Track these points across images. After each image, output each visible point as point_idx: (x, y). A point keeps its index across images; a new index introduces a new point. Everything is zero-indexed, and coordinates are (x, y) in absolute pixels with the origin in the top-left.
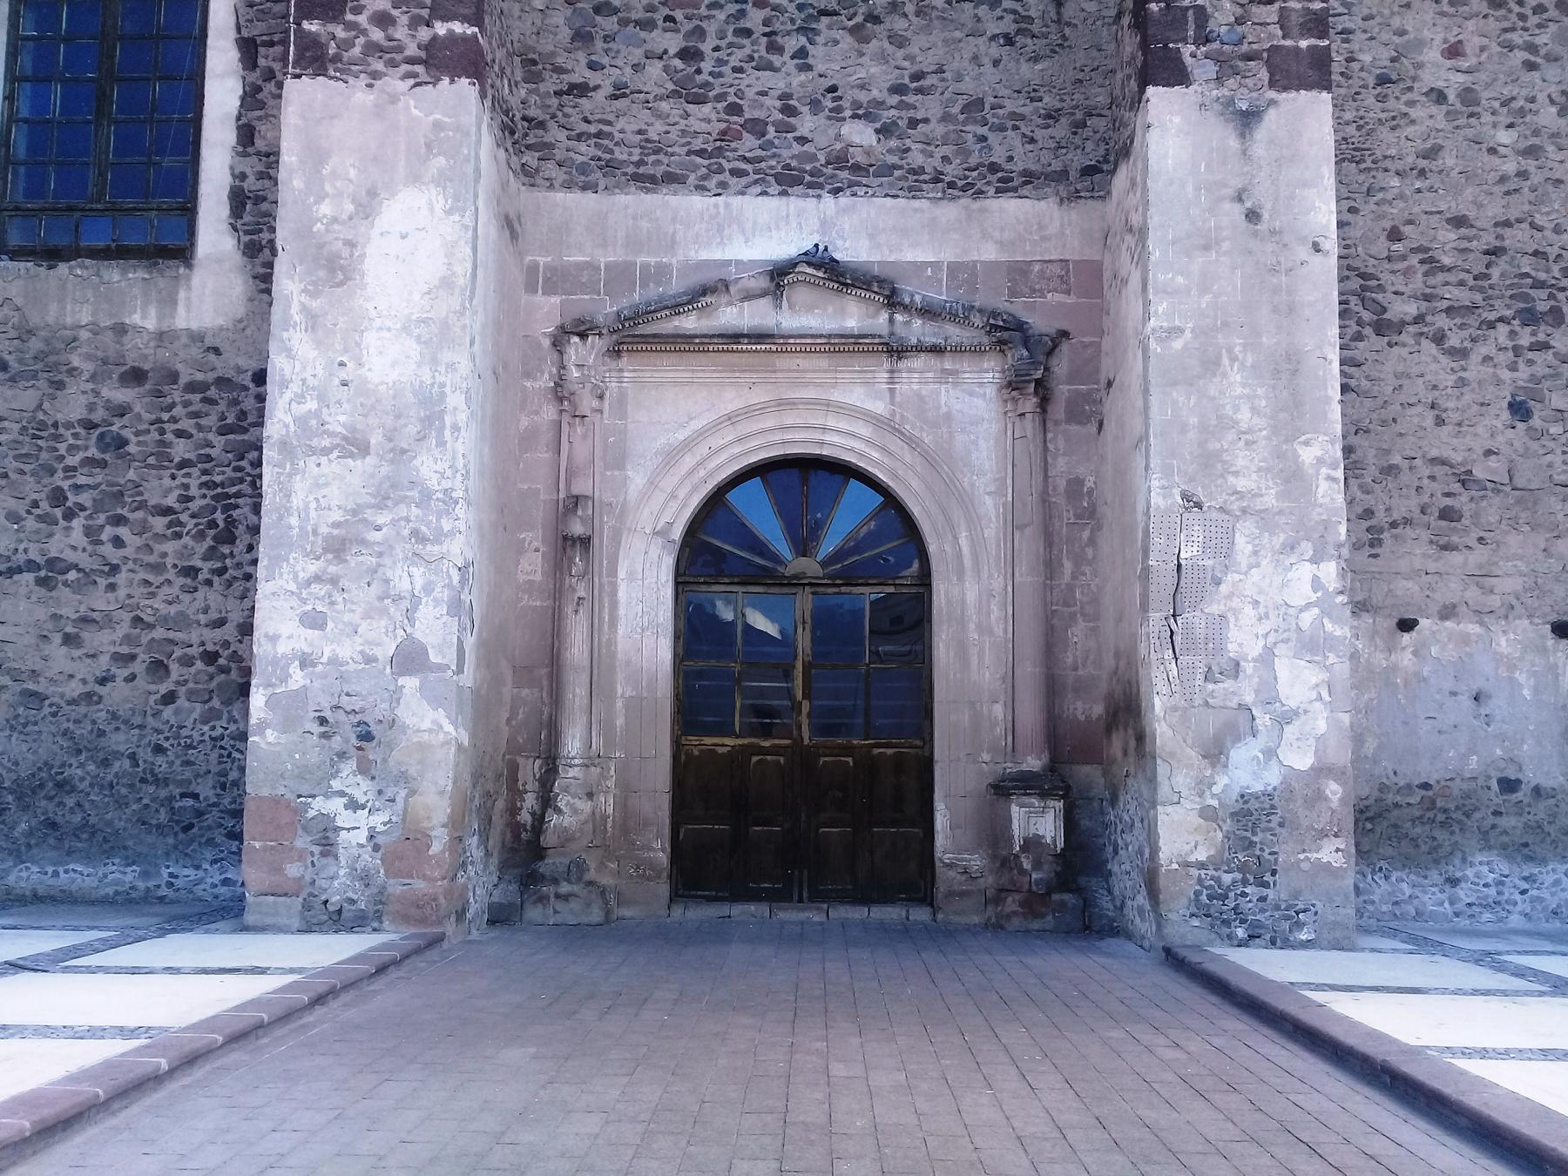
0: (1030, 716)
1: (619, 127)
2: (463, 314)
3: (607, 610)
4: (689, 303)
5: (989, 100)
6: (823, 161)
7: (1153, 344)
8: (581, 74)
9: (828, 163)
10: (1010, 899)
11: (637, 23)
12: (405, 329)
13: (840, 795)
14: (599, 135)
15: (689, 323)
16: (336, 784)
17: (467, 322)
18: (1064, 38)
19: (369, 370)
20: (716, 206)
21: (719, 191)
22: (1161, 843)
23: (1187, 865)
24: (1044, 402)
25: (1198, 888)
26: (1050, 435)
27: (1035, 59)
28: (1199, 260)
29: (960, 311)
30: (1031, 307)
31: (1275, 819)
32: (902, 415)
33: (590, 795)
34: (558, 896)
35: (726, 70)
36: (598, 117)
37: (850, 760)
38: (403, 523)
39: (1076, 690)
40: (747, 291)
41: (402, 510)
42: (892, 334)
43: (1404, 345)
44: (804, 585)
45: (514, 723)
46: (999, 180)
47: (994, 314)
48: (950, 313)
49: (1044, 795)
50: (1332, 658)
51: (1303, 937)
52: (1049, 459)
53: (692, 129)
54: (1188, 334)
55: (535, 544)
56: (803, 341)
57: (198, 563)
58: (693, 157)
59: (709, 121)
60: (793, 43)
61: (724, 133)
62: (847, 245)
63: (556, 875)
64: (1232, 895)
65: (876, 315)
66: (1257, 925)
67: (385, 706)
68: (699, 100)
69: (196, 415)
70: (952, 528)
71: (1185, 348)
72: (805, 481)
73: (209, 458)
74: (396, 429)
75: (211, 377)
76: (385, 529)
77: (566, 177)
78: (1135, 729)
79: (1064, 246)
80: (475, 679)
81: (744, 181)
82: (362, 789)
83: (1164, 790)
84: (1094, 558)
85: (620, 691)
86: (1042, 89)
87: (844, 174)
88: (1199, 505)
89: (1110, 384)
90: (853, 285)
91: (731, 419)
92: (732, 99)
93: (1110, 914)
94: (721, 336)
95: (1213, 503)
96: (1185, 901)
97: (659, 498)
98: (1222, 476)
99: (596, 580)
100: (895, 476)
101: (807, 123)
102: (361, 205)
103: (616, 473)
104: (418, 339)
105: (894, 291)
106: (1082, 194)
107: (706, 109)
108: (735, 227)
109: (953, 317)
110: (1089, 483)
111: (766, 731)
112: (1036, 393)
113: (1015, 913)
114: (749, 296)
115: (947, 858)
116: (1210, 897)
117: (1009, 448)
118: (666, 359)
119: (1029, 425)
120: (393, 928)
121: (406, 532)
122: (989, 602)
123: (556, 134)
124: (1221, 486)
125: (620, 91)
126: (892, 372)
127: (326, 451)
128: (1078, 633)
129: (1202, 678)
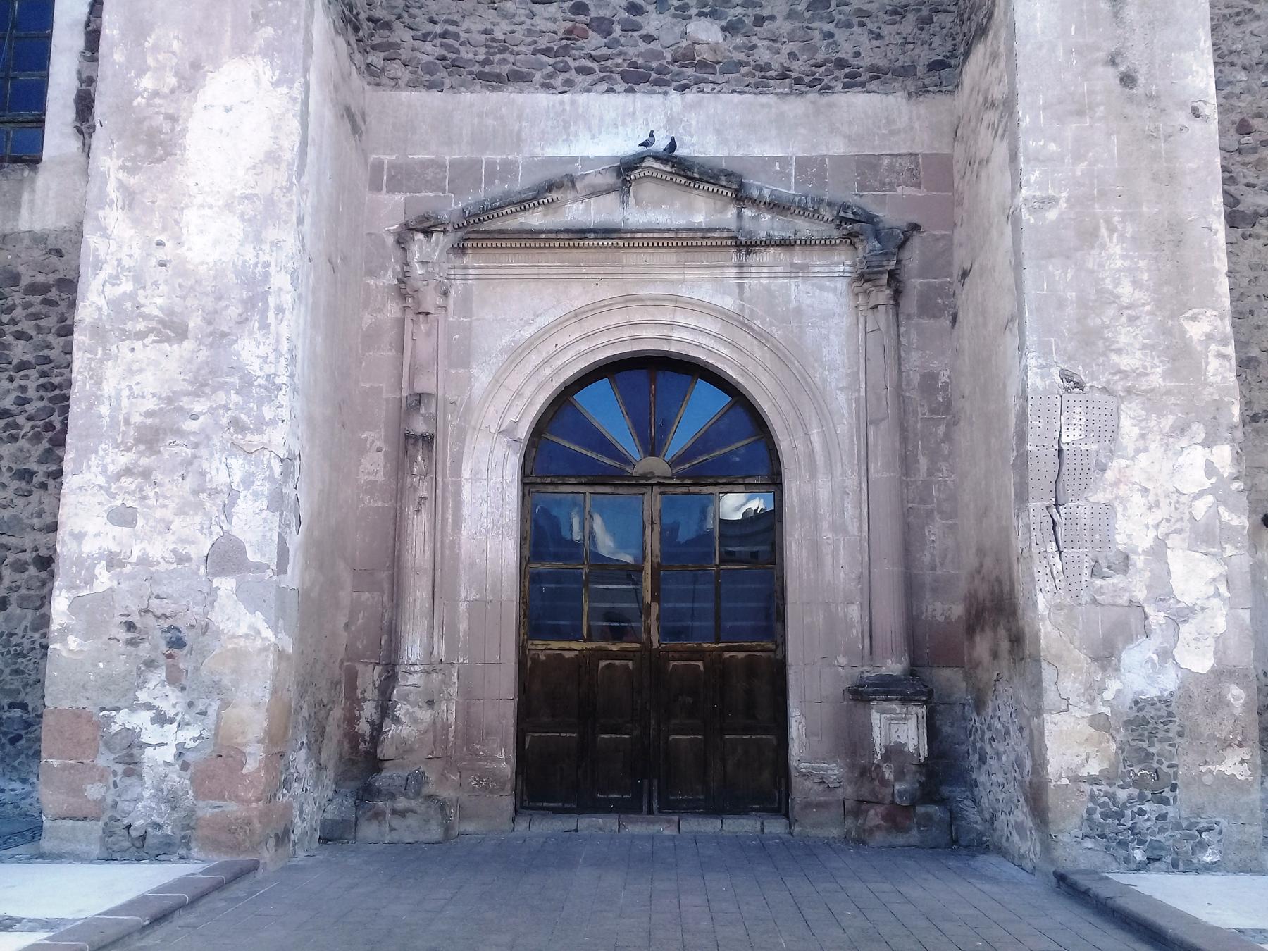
0: (889, 619)
1: (464, 26)
2: (289, 190)
4: (534, 198)
6: (669, 59)
7: (1025, 215)
10: (872, 812)
12: (229, 206)
13: (690, 700)
14: (445, 35)
15: (534, 219)
16: (143, 696)
17: (294, 198)
19: (189, 249)
20: (562, 103)
21: (566, 88)
22: (1049, 755)
23: (1077, 780)
24: (897, 294)
25: (1091, 805)
26: (902, 329)
28: (1071, 128)
29: (810, 205)
30: (881, 201)
31: (1174, 728)
32: (752, 311)
33: (431, 704)
34: (394, 812)
37: (700, 664)
38: (221, 412)
39: (934, 590)
40: (593, 186)
41: (221, 398)
43: (1258, 237)
44: (652, 485)
45: (353, 628)
46: (847, 76)
47: (845, 207)
48: (799, 207)
49: (906, 700)
50: (1230, 550)
51: (1208, 858)
52: (903, 355)
54: (1063, 204)
55: (378, 444)
56: (651, 235)
57: (33, 466)
58: (539, 56)
59: (555, 21)
62: (695, 140)
63: (393, 790)
64: (1128, 812)
65: (723, 210)
66: (1159, 846)
67: (198, 609)
69: (36, 317)
70: (804, 425)
71: (1060, 219)
73: (48, 360)
74: (216, 312)
75: (51, 278)
76: (202, 419)
77: (411, 76)
78: (1009, 630)
79: (913, 140)
80: (303, 583)
81: (590, 78)
82: (171, 701)
83: (1050, 697)
84: (951, 453)
85: (463, 595)
87: (690, 71)
88: (1080, 386)
89: (965, 274)
90: (701, 180)
91: (578, 316)
93: (979, 827)
94: (567, 231)
95: (1095, 383)
96: (1076, 821)
97: (504, 396)
98: (1104, 354)
99: (440, 479)
100: (743, 370)
102: (184, 78)
103: (462, 371)
104: (242, 214)
105: (742, 186)
109: (803, 211)
110: (944, 376)
111: (617, 634)
112: (889, 285)
113: (878, 827)
114: (595, 192)
115: (804, 767)
116: (1105, 816)
117: (861, 343)
118: (511, 258)
119: (883, 318)
120: (202, 855)
121: (225, 421)
122: (842, 499)
123: (401, 34)
124: (1103, 364)
126: (741, 266)
127: (140, 336)
128: (935, 531)
129: (1088, 573)
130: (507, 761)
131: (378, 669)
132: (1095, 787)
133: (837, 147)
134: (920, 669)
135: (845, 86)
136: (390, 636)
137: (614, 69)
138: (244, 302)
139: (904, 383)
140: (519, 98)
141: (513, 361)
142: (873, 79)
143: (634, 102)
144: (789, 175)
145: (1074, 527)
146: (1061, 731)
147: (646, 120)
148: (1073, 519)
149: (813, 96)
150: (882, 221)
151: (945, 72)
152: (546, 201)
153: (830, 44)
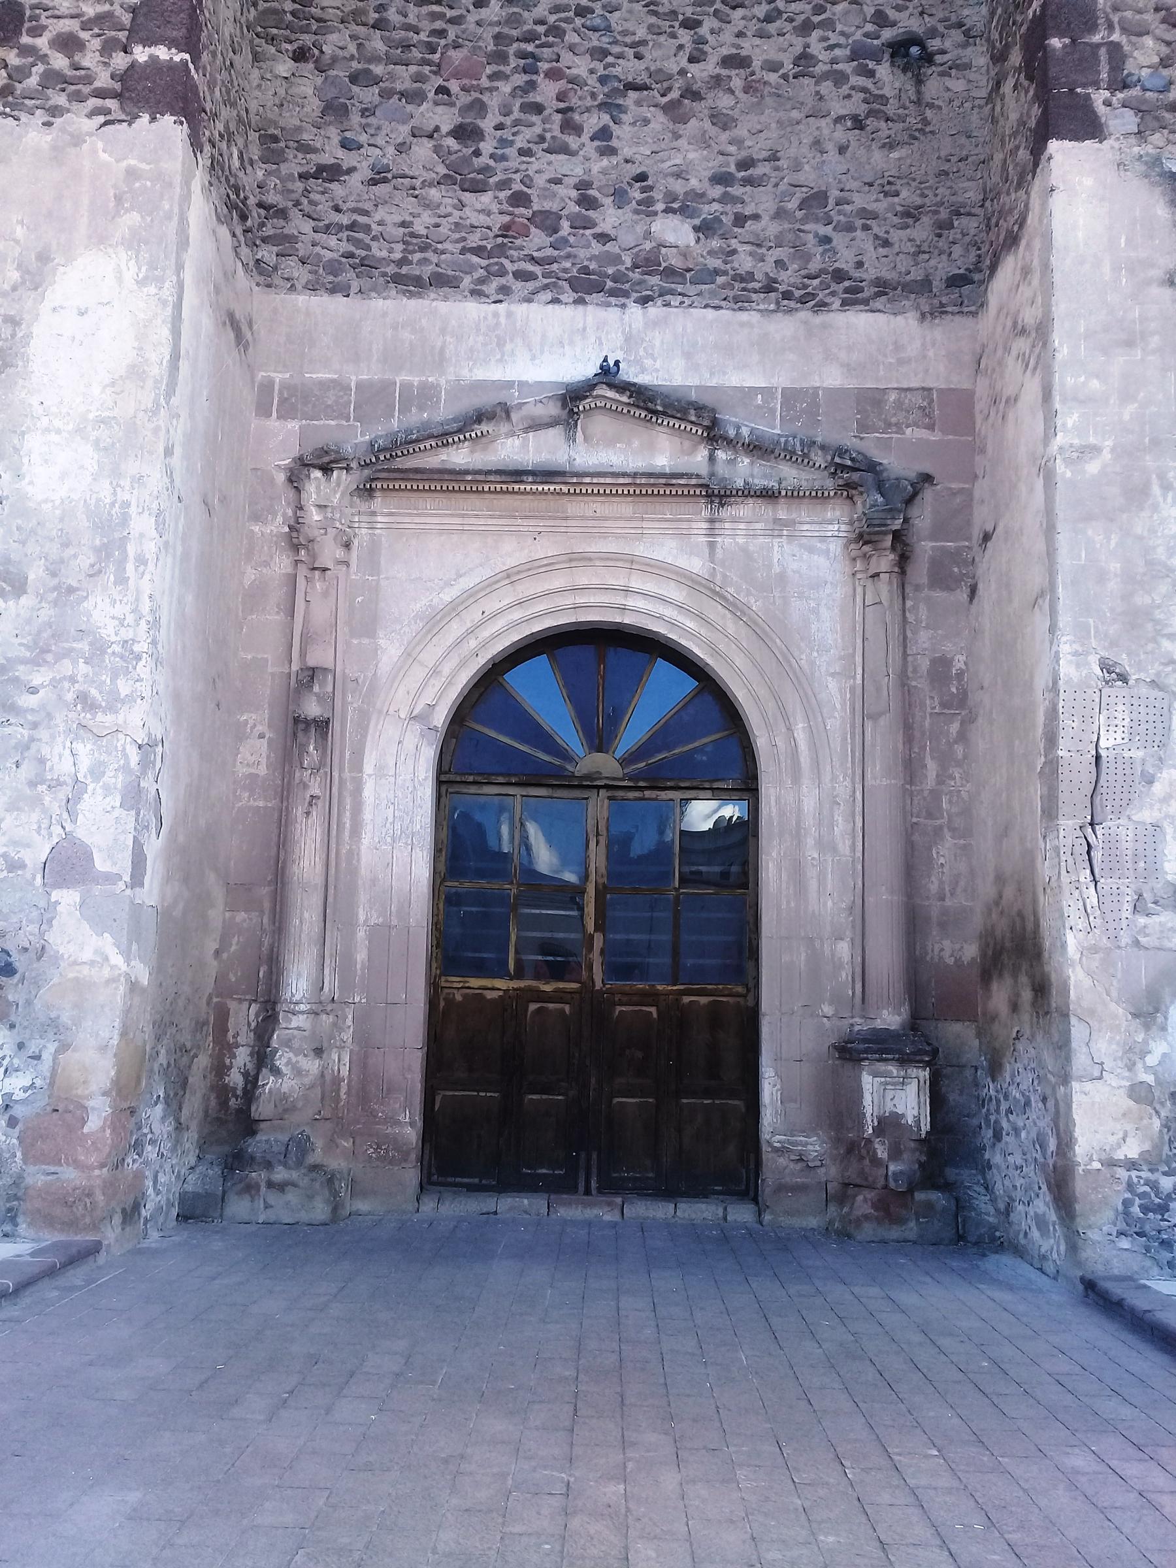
1: (377, 217)
2: (155, 412)
3: (348, 814)
4: (460, 431)
5: (834, 194)
6: (629, 264)
7: (1060, 468)
8: (332, 153)
9: (635, 266)
10: (860, 1198)
11: (402, 94)
12: (79, 431)
13: (639, 1054)
14: (353, 226)
15: (459, 456)
17: (161, 423)
18: (926, 122)
19: (31, 483)
20: (496, 315)
21: (501, 297)
22: (1077, 1133)
23: (1111, 1163)
24: (903, 560)
25: (1128, 1195)
26: (909, 603)
27: (890, 145)
28: (1120, 361)
29: (798, 448)
30: (886, 445)
32: (725, 576)
33: (319, 1052)
34: (270, 1185)
35: (511, 152)
36: (352, 205)
37: (653, 1010)
38: (66, 685)
39: (943, 925)
40: (533, 419)
41: (66, 667)
42: (712, 474)
44: (598, 787)
45: (225, 956)
46: (847, 290)
47: (841, 451)
48: (785, 449)
49: (904, 1061)
52: (909, 634)
53: (468, 222)
54: (1107, 455)
55: (260, 728)
56: (602, 480)
58: (468, 256)
59: (489, 214)
60: (593, 121)
61: (506, 228)
62: (658, 365)
63: (268, 1157)
65: (694, 449)
67: (33, 928)
68: (477, 188)
70: (785, 717)
72: (601, 659)
74: (62, 561)
76: (42, 692)
77: (311, 277)
78: (1032, 977)
79: (927, 371)
80: (163, 897)
81: (531, 285)
83: (1080, 1061)
84: (965, 757)
85: (362, 918)
86: (899, 182)
87: (654, 280)
88: (1123, 678)
89: (987, 537)
90: (664, 413)
91: (511, 576)
92: (518, 186)
93: (991, 1219)
94: (499, 472)
95: (1142, 676)
96: (1110, 1214)
97: (418, 674)
98: (1154, 640)
99: (336, 774)
100: (714, 650)
101: (609, 218)
102: (28, 272)
103: (366, 641)
104: (97, 442)
105: (715, 422)
106: (949, 309)
107: (486, 198)
108: (519, 341)
109: (789, 455)
110: (959, 662)
112: (893, 548)
113: (867, 1217)
114: (535, 426)
116: (1145, 1209)
117: (859, 618)
118: (429, 503)
119: (885, 589)
120: (31, 1233)
121: (70, 697)
122: (832, 810)
123: (300, 225)
124: (1152, 652)
125: (379, 177)
126: (712, 521)
128: (944, 852)
129: (1131, 908)
130: (412, 1124)
131: (254, 1008)
132: (1134, 1174)
133: (832, 378)
134: (924, 1022)
135: (845, 303)
136: (270, 968)
137: (561, 275)
138: (97, 550)
139: (910, 669)
140: (443, 307)
141: (429, 631)
142: (879, 294)
143: (585, 315)
144: (772, 411)
145: (1114, 850)
146: (1093, 1103)
147: (600, 339)
148: (1112, 842)
149: (804, 315)
150: (886, 470)
151: (966, 289)
152: (473, 435)
153: (826, 251)
